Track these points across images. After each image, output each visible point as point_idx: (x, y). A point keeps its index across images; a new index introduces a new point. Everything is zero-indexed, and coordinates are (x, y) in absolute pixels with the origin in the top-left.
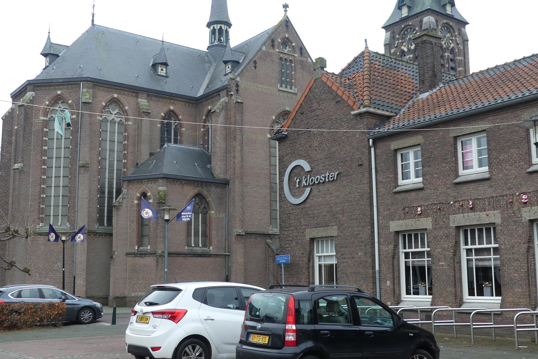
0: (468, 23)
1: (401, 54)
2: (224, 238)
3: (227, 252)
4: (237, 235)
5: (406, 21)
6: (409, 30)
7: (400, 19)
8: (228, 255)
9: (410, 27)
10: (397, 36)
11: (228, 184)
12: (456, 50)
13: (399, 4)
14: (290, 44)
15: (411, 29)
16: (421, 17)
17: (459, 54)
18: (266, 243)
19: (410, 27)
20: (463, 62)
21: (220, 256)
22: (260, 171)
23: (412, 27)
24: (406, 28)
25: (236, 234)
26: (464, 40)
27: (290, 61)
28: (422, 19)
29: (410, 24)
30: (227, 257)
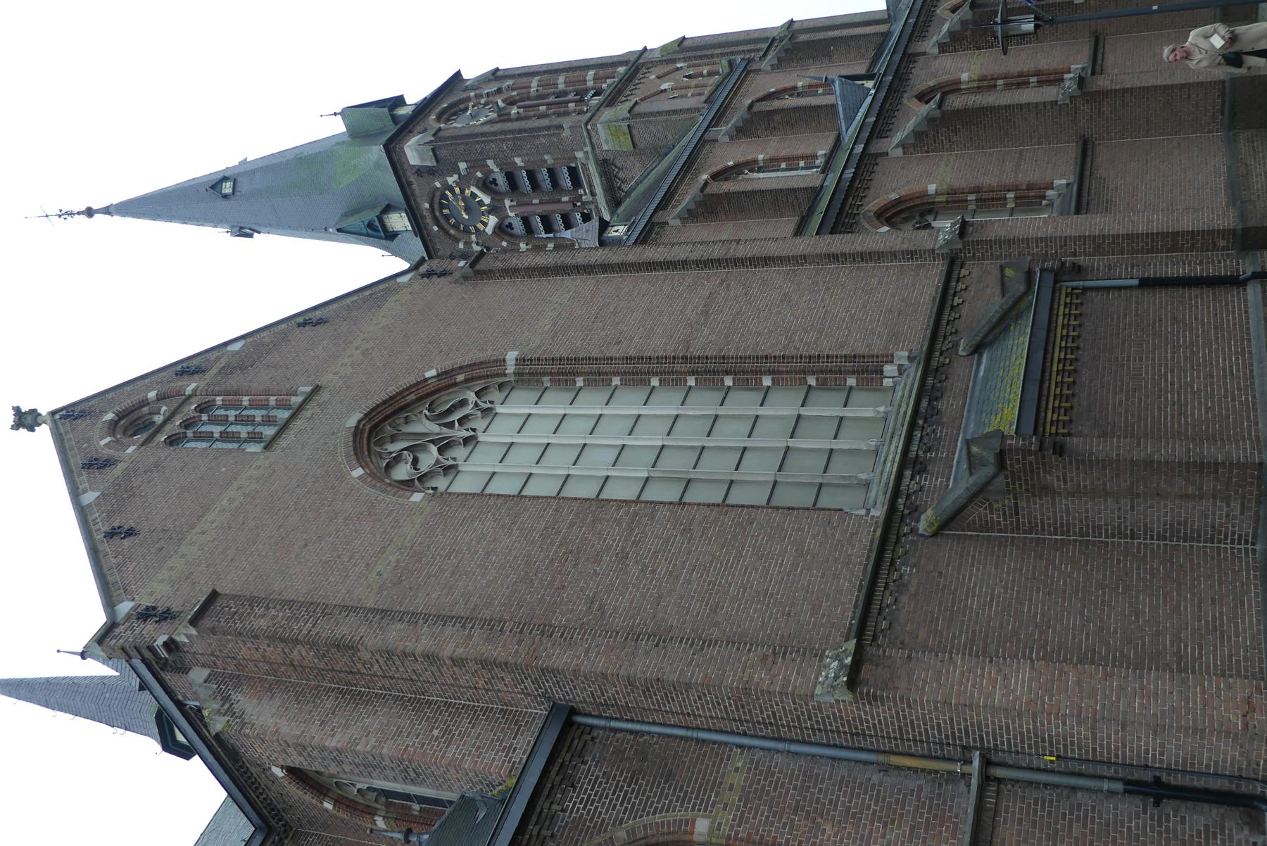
0: (458, 74)
1: (506, 237)
2: (876, 778)
3: (967, 769)
4: (852, 684)
5: (423, 217)
6: (446, 211)
7: (416, 236)
8: (987, 763)
9: (436, 206)
10: (461, 246)
11: (573, 711)
12: (514, 93)
13: (380, 238)
14: (146, 410)
15: (442, 206)
16: (409, 173)
17: (526, 87)
18: (935, 535)
19: (436, 206)
20: (546, 76)
21: (987, 818)
22: (552, 544)
23: (437, 200)
24: (442, 220)
25: (849, 697)
26: (492, 77)
27: (201, 409)
28: (415, 170)
29: (427, 205)
30: (999, 772)
